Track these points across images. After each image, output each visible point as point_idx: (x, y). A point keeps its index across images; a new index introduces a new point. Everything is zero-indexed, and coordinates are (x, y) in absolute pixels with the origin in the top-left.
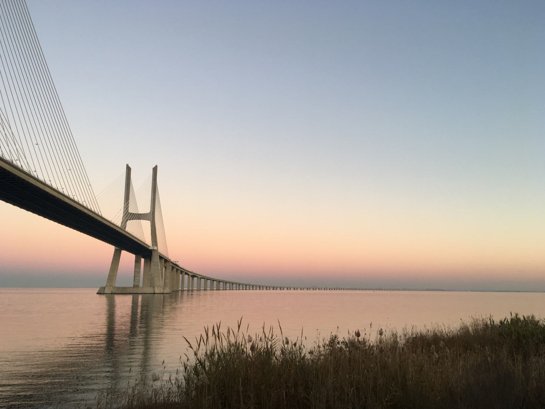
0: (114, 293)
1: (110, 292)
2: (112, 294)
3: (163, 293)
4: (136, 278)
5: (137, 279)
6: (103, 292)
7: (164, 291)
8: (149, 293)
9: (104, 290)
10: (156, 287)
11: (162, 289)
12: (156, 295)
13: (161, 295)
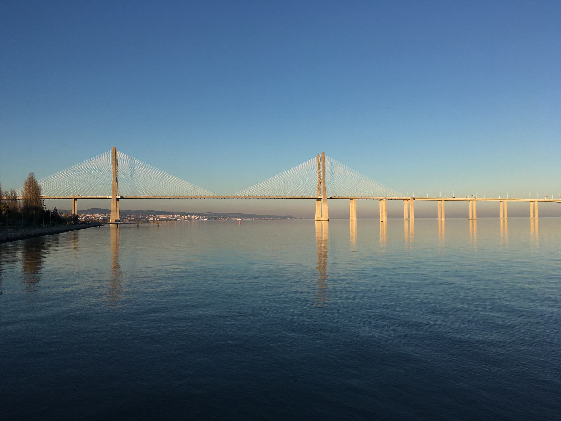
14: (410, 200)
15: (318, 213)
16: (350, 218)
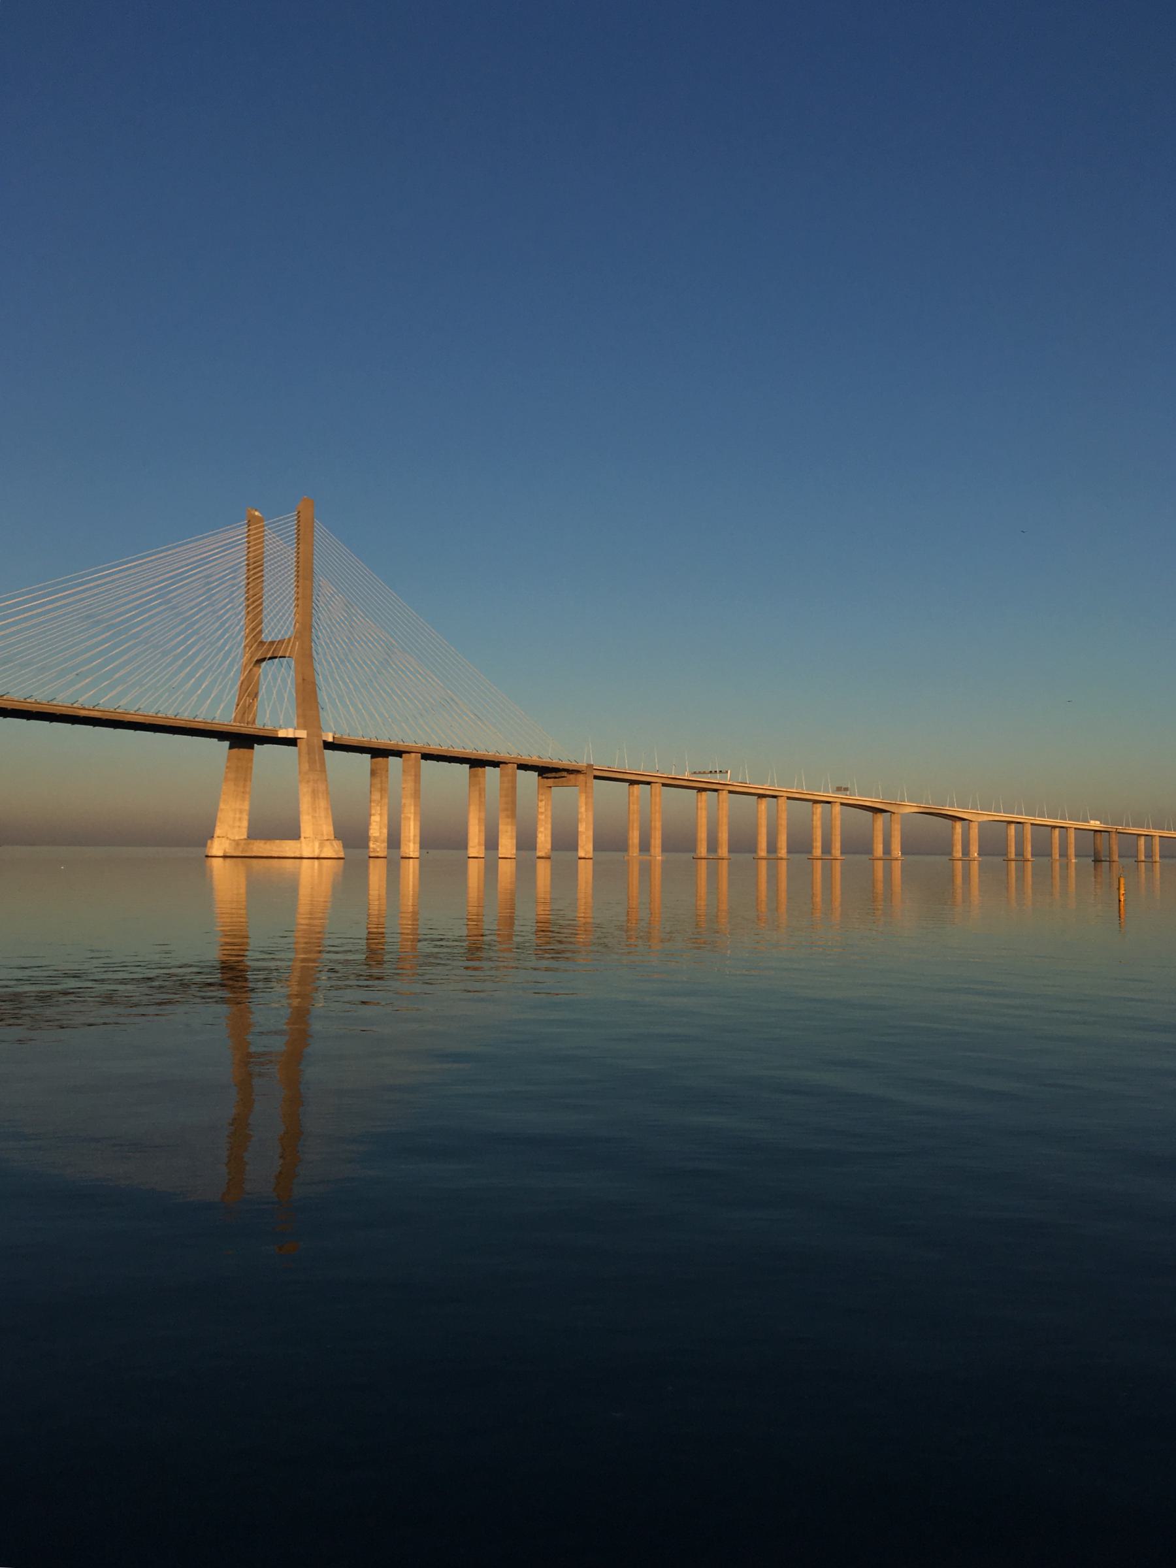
0: (228, 855)
1: (221, 854)
2: (225, 857)
3: (317, 858)
7: (321, 851)
8: (293, 855)
11: (317, 844)
13: (316, 861)
14: (581, 777)
15: (238, 816)
16: (372, 845)
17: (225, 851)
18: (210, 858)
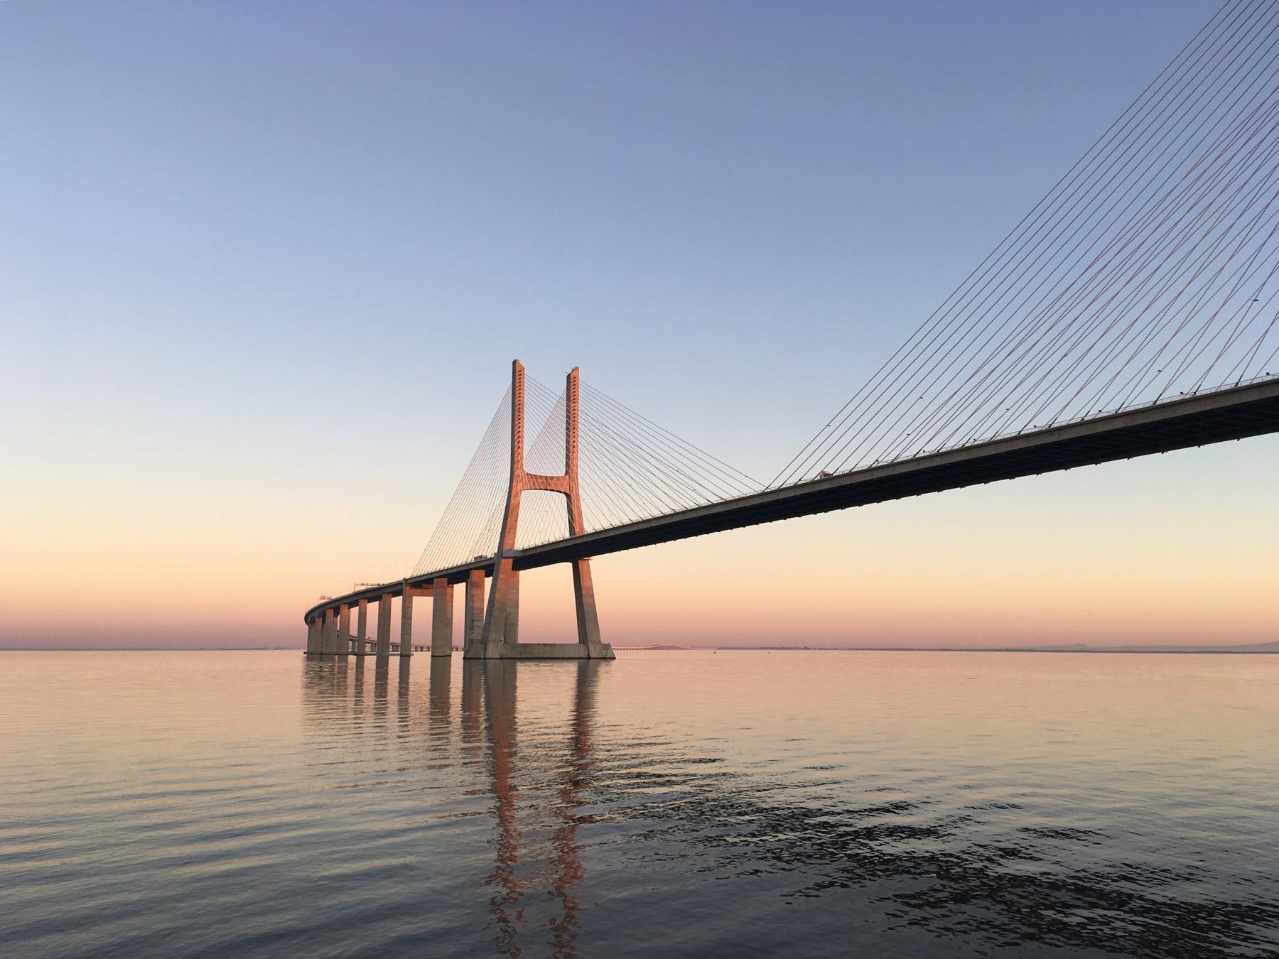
0: (504, 657)
2: (501, 659)
4: (475, 623)
5: (479, 627)
6: (482, 657)
7: (607, 654)
8: (578, 656)
9: (485, 649)
10: (590, 643)
12: (591, 661)
17: (502, 655)
18: (482, 661)
